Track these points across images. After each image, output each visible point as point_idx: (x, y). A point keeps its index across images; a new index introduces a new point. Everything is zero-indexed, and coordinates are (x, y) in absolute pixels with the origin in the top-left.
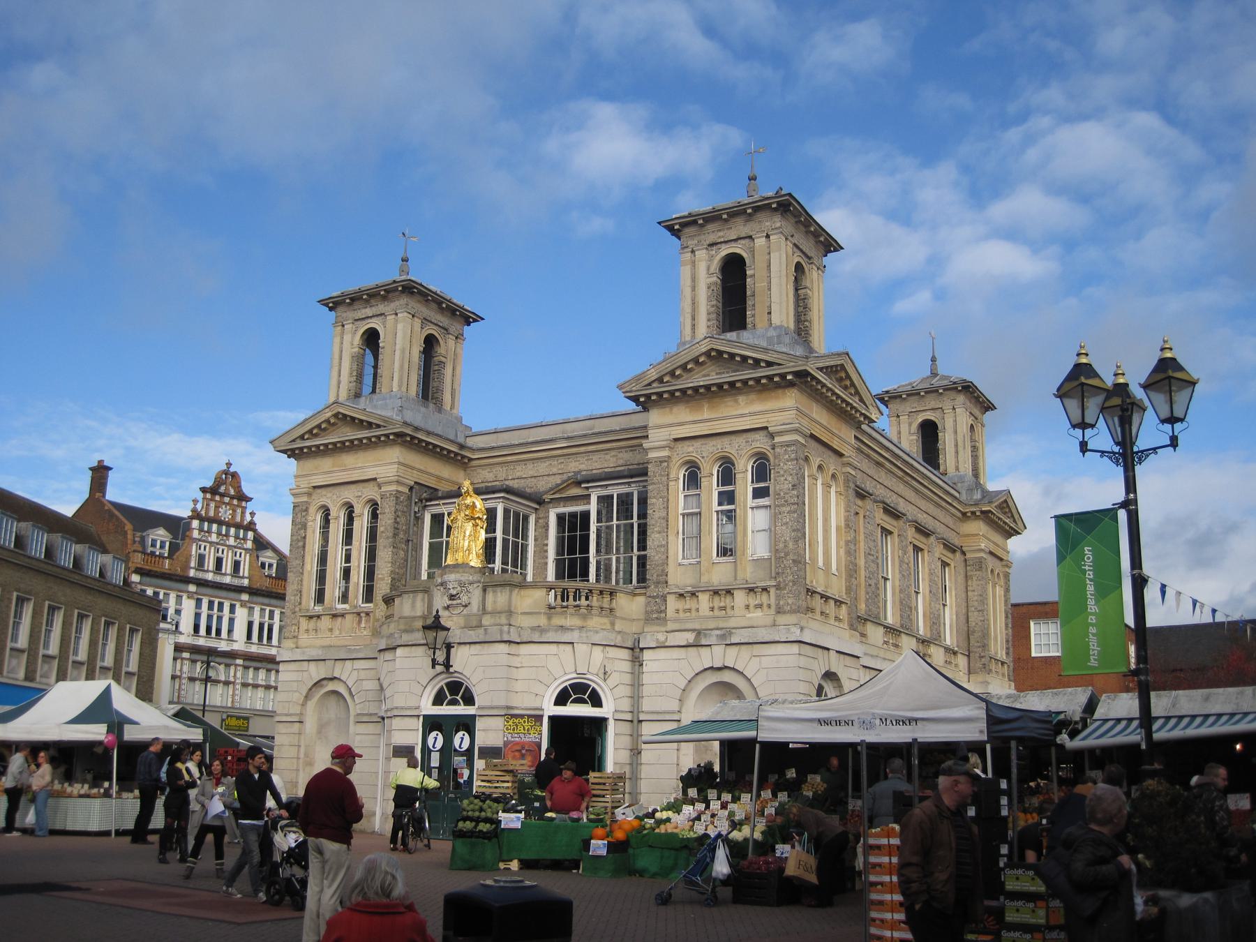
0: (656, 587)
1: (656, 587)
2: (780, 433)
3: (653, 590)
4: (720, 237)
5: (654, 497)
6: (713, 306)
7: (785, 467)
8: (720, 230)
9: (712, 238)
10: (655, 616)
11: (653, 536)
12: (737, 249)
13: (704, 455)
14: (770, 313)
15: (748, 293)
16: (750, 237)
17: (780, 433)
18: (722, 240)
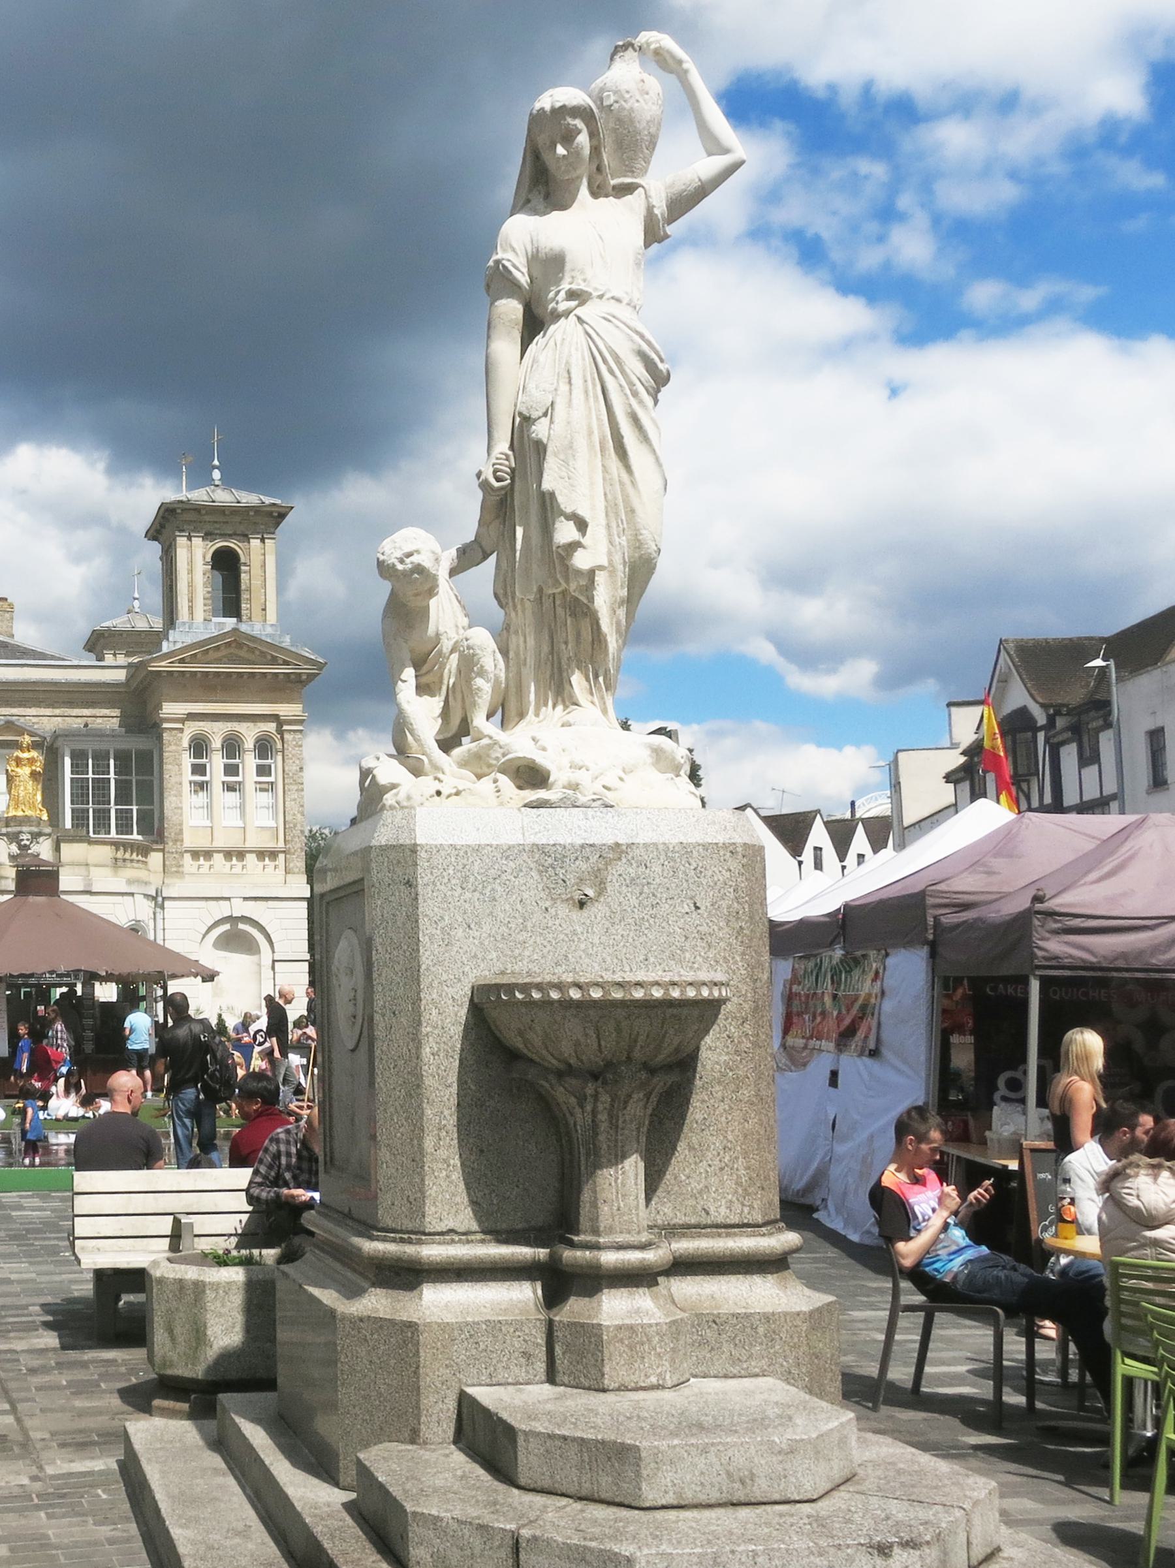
0: (175, 844)
1: (175, 844)
2: (290, 723)
3: (170, 846)
4: (216, 529)
5: (170, 764)
6: (208, 592)
7: (293, 752)
8: (216, 522)
9: (208, 527)
10: (174, 869)
11: (170, 798)
12: (231, 544)
13: (215, 730)
14: (264, 610)
15: (243, 587)
16: (246, 536)
17: (290, 723)
18: (218, 532)
